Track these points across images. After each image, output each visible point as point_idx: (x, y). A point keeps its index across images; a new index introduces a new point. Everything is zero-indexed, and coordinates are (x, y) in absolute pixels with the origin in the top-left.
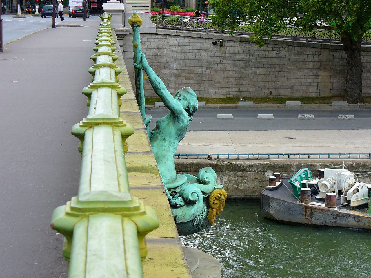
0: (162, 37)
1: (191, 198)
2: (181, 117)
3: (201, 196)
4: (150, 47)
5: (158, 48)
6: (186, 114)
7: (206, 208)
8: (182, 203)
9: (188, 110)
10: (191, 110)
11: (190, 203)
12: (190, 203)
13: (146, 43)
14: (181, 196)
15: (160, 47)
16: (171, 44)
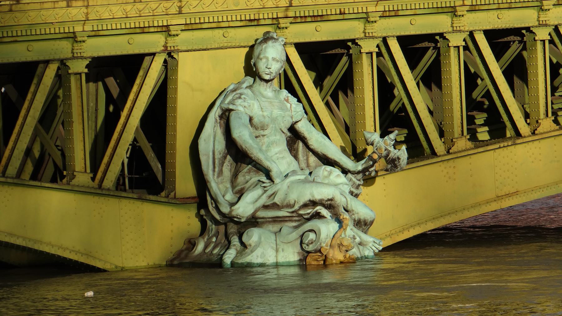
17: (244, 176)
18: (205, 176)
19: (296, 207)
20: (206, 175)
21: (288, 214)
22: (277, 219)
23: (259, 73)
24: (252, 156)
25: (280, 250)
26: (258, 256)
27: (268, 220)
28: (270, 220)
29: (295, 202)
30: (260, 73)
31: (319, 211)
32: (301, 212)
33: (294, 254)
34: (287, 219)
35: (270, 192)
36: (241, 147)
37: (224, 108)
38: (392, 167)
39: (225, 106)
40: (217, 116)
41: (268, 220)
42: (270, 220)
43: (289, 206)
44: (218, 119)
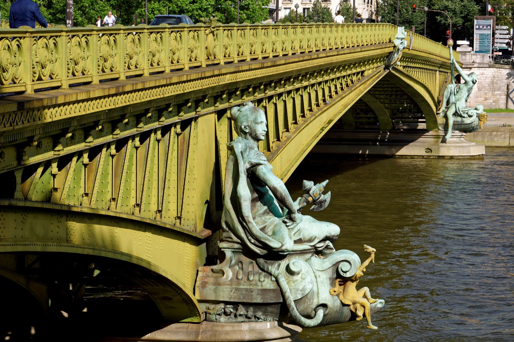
0: (497, 70)
1: (471, 114)
2: (469, 83)
3: (475, 115)
4: (488, 76)
5: (494, 77)
6: (471, 83)
7: (478, 120)
8: (467, 116)
9: (473, 82)
10: (474, 81)
11: (470, 116)
12: (470, 116)
13: (486, 74)
14: (467, 113)
15: (495, 76)
16: (502, 74)
17: (260, 217)
18: (246, 219)
19: (316, 241)
20: (247, 217)
21: (310, 248)
22: (303, 252)
23: (256, 135)
24: (288, 202)
25: (317, 276)
26: (309, 283)
27: (297, 252)
28: (299, 252)
29: (315, 238)
30: (258, 135)
31: (329, 244)
32: (318, 245)
33: (327, 280)
34: (308, 251)
35: (296, 230)
36: (281, 194)
37: (253, 163)
38: (318, 207)
39: (254, 161)
40: (245, 169)
41: (297, 252)
42: (299, 252)
43: (310, 240)
44: (246, 171)
